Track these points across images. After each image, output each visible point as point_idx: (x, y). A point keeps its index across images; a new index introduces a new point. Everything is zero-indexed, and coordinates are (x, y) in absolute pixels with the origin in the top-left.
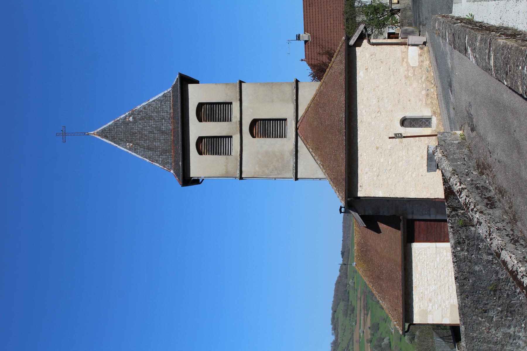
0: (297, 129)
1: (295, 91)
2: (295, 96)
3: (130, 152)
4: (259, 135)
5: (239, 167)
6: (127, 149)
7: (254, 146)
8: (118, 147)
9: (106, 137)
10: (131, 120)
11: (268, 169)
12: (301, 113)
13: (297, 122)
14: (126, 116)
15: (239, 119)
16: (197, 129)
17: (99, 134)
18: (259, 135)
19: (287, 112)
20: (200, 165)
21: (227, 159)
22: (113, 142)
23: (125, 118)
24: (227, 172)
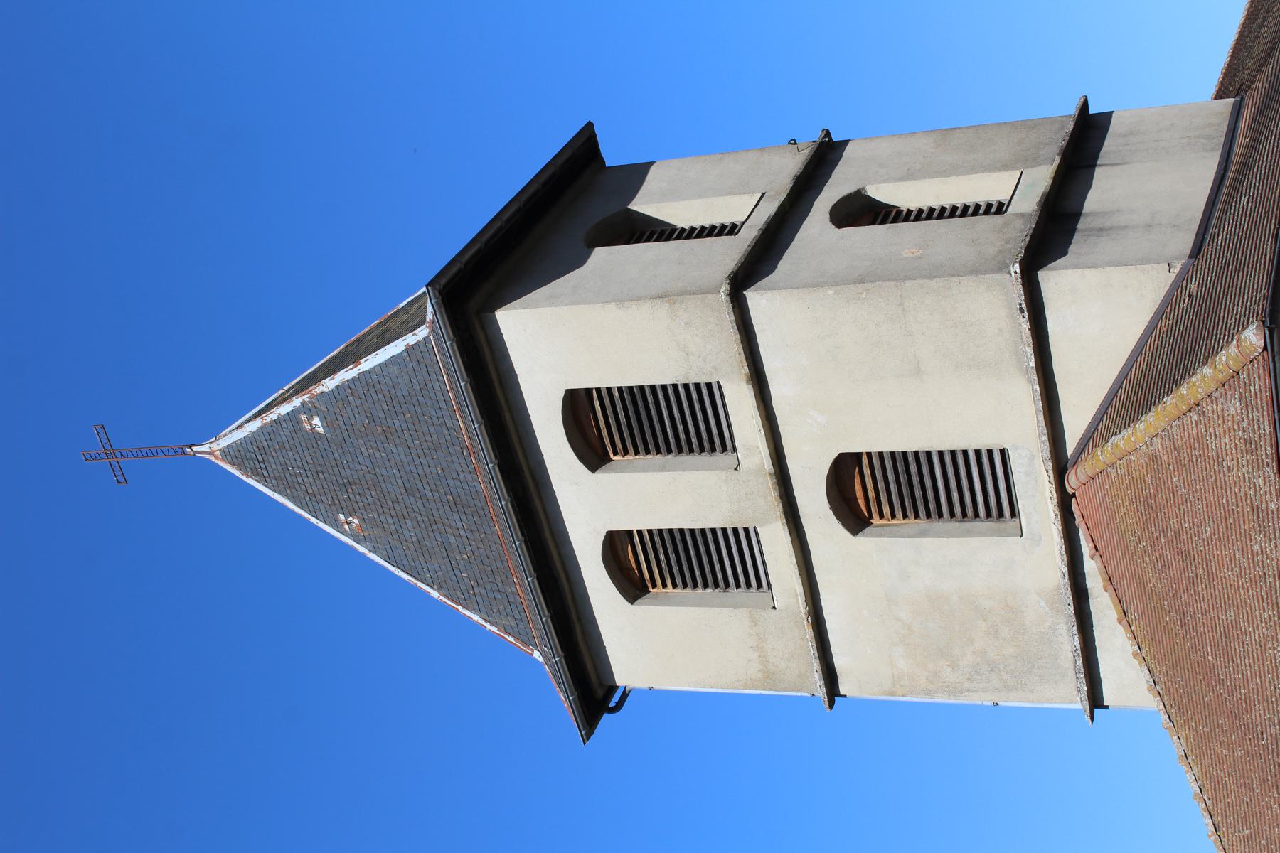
0: (1065, 501)
1: (1025, 325)
2: (1030, 351)
3: (361, 549)
4: (886, 509)
5: (816, 665)
6: (344, 533)
7: (873, 574)
8: (314, 520)
9: (254, 473)
10: (321, 430)
11: (954, 666)
12: (1075, 426)
13: (1061, 466)
14: (295, 412)
15: (768, 466)
16: (594, 504)
17: (227, 453)
18: (886, 509)
19: (995, 415)
20: (643, 640)
21: (755, 622)
22: (287, 496)
23: (293, 416)
24: (769, 677)
